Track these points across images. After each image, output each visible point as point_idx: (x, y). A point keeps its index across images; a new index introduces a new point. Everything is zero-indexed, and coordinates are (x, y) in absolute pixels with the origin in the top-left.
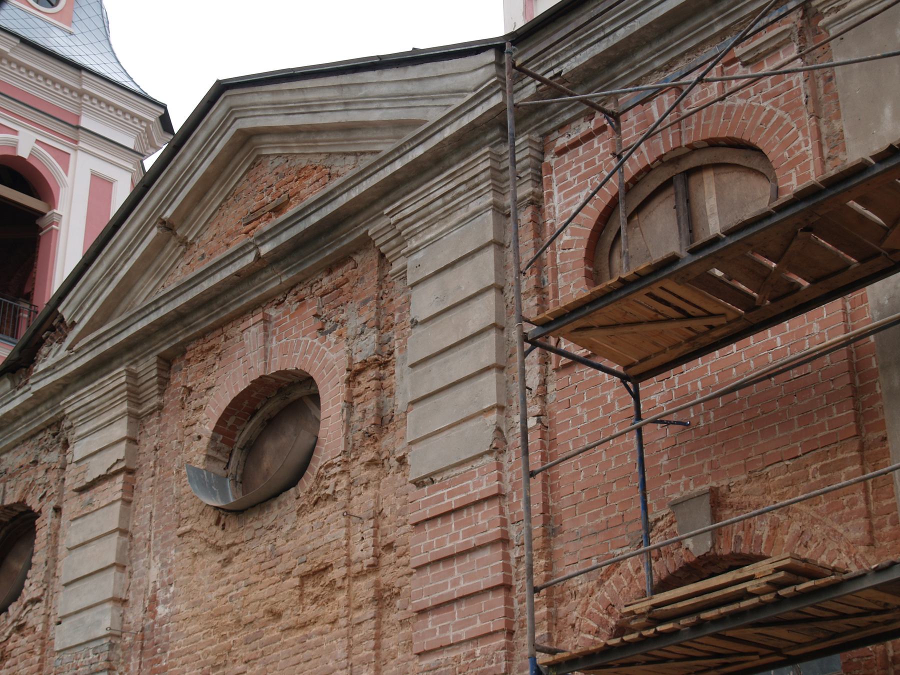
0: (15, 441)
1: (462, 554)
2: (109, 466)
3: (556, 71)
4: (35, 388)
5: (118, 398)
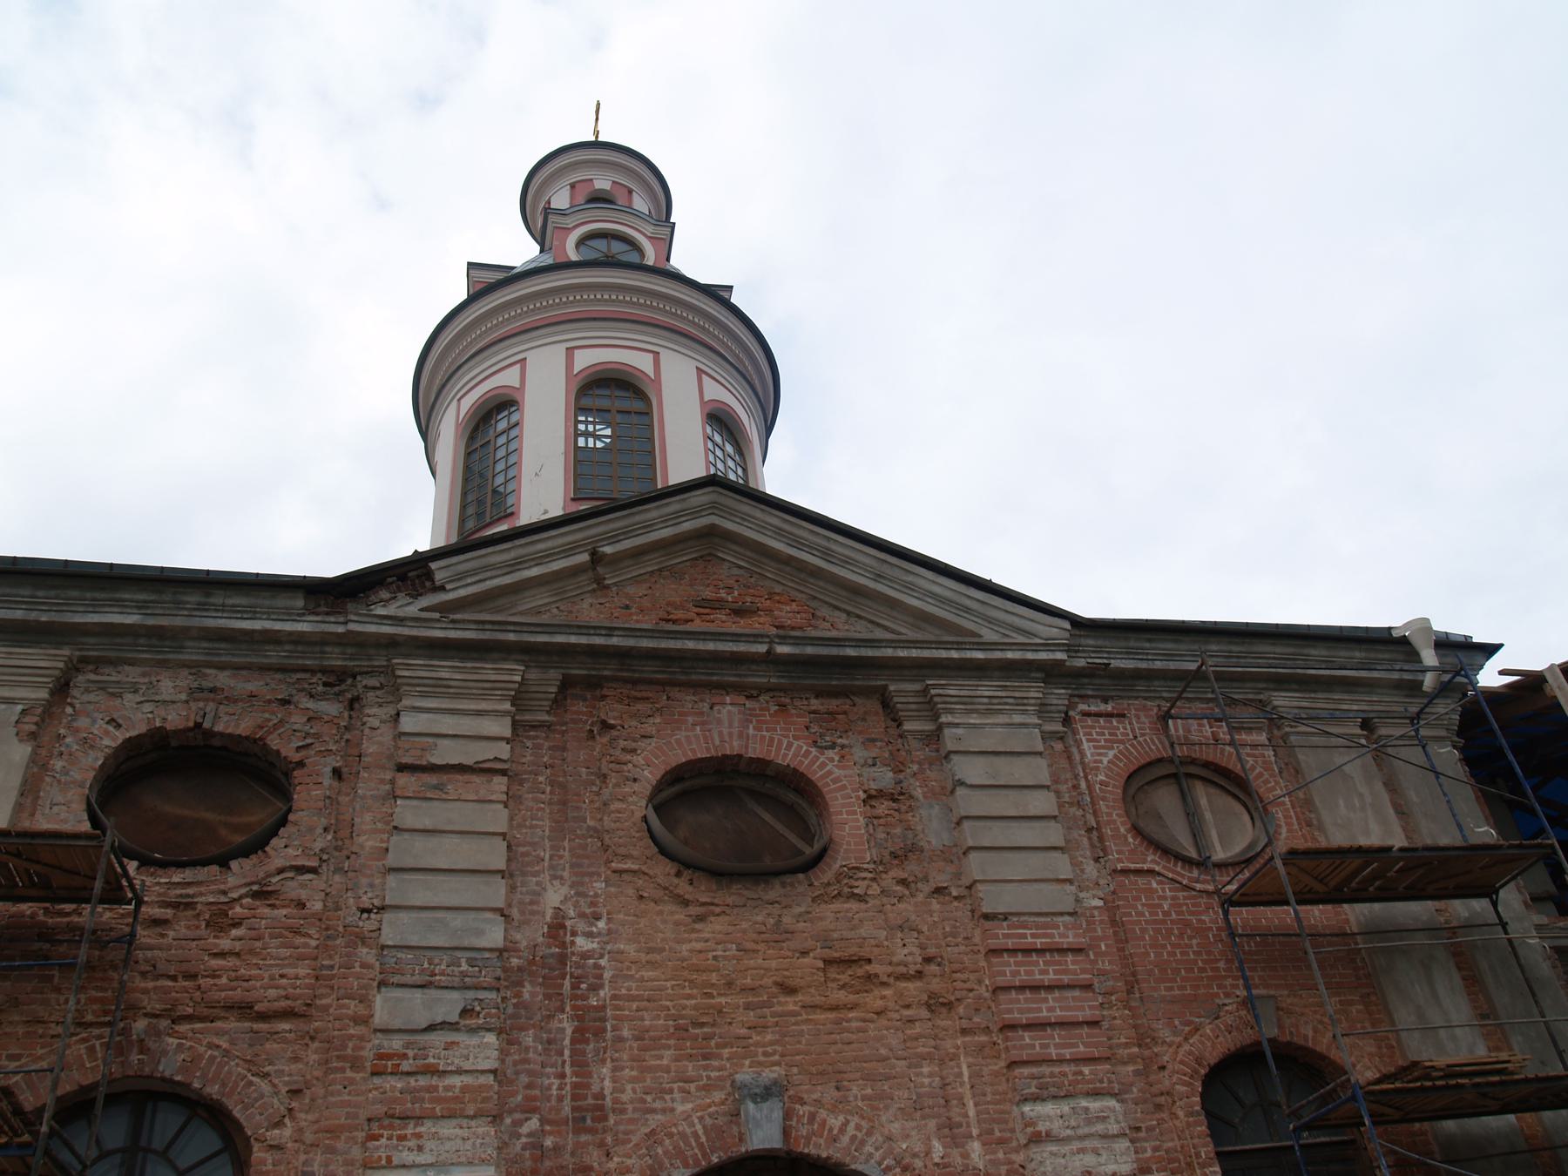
0: (250, 663)
1: (1050, 988)
3: (1105, 661)
4: (352, 627)
5: (499, 692)
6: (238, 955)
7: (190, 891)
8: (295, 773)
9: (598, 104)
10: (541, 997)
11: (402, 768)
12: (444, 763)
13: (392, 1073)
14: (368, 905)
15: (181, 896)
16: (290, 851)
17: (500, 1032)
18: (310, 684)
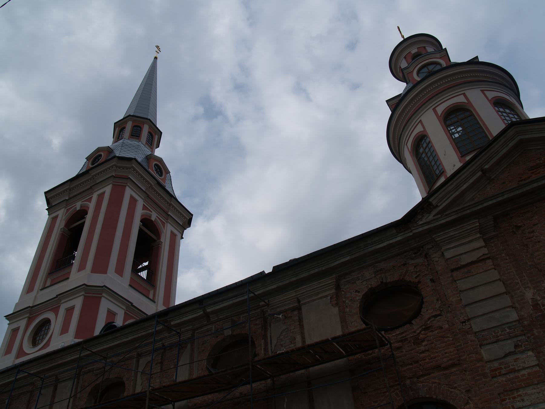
2: (478, 257)
4: (415, 231)
5: (473, 232)
6: (428, 351)
7: (404, 335)
8: (419, 286)
9: (398, 28)
10: (542, 333)
11: (453, 270)
12: (466, 263)
13: (499, 376)
14: (463, 320)
15: (402, 337)
16: (429, 311)
17: (533, 350)
18: (410, 255)
